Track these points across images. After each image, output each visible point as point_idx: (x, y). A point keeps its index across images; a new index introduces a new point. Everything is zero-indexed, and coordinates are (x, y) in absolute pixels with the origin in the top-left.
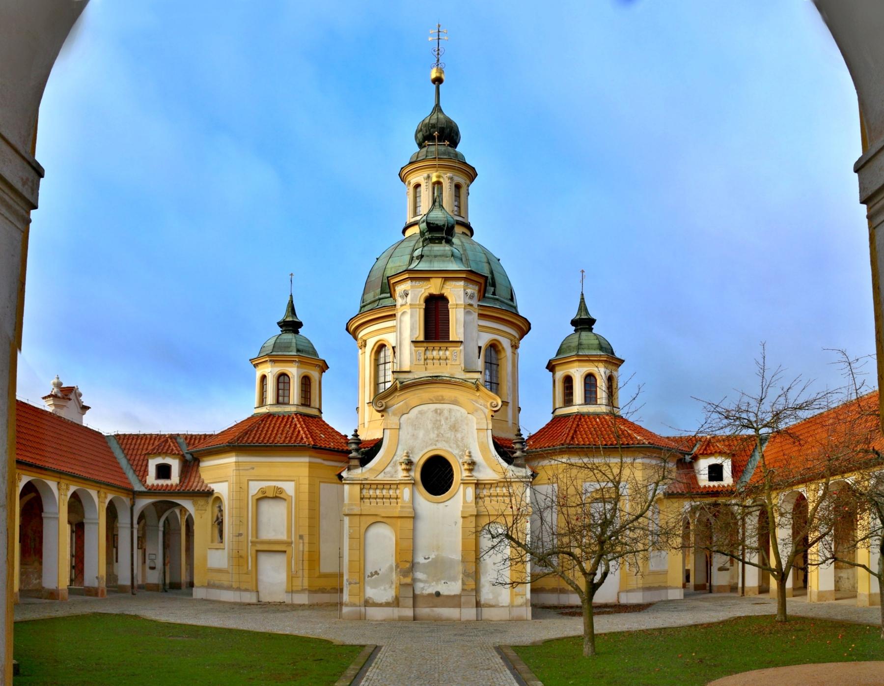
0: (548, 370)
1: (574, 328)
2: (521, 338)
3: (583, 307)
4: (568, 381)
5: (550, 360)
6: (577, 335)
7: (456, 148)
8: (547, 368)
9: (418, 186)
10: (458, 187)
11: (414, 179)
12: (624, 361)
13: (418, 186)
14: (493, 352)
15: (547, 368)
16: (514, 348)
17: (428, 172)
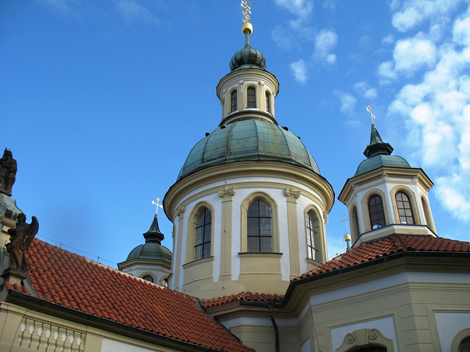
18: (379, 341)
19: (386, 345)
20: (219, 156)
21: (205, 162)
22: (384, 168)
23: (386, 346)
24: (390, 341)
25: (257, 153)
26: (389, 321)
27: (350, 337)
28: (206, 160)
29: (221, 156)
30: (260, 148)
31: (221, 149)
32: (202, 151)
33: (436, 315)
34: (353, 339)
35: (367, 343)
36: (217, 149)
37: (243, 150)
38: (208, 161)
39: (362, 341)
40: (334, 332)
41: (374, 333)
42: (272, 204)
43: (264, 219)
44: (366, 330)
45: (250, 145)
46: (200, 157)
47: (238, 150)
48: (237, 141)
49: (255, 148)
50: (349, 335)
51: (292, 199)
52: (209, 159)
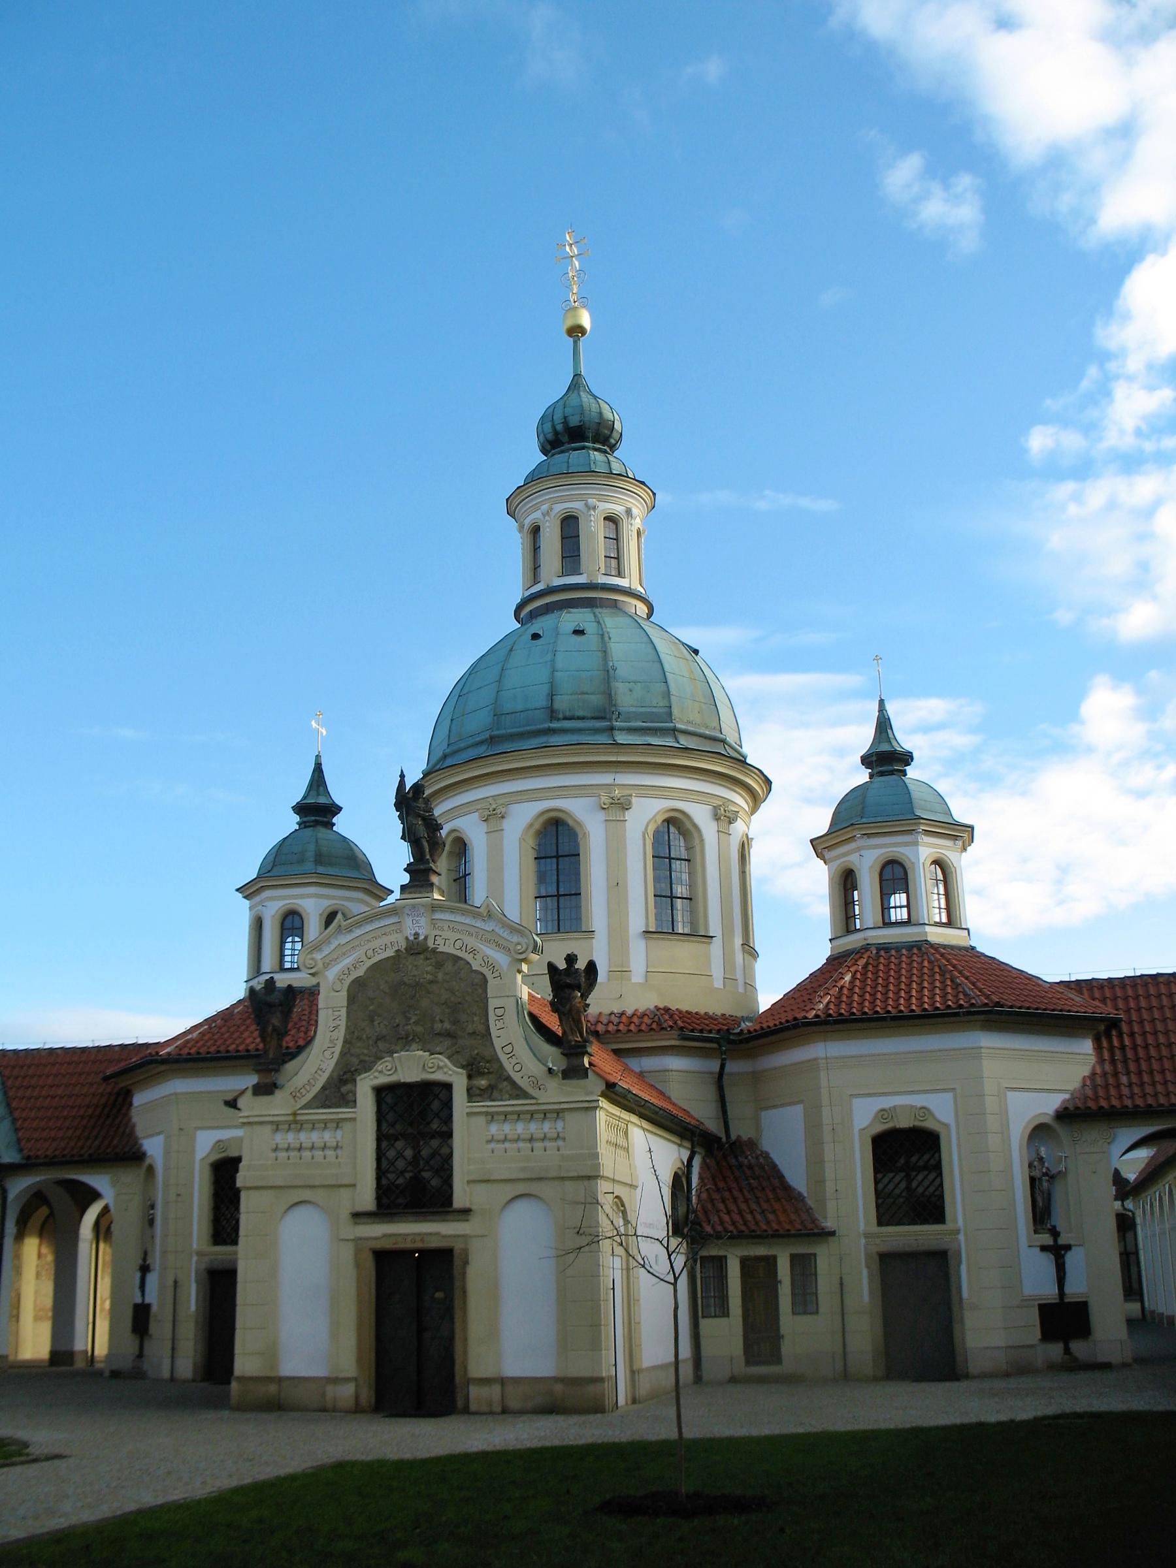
18: (929, 1125)
19: (940, 1130)
21: (559, 720)
22: (922, 821)
23: (939, 1132)
24: (947, 1126)
27: (883, 1114)
28: (561, 716)
29: (597, 714)
30: (676, 712)
31: (593, 697)
32: (544, 690)
33: (1010, 1094)
34: (890, 1116)
35: (912, 1126)
38: (565, 718)
39: (904, 1123)
40: (857, 1103)
41: (924, 1113)
42: (695, 835)
43: (678, 862)
44: (912, 1107)
45: (656, 703)
46: (542, 702)
47: (633, 709)
49: (666, 710)
50: (883, 1110)
51: (724, 824)
52: (568, 714)
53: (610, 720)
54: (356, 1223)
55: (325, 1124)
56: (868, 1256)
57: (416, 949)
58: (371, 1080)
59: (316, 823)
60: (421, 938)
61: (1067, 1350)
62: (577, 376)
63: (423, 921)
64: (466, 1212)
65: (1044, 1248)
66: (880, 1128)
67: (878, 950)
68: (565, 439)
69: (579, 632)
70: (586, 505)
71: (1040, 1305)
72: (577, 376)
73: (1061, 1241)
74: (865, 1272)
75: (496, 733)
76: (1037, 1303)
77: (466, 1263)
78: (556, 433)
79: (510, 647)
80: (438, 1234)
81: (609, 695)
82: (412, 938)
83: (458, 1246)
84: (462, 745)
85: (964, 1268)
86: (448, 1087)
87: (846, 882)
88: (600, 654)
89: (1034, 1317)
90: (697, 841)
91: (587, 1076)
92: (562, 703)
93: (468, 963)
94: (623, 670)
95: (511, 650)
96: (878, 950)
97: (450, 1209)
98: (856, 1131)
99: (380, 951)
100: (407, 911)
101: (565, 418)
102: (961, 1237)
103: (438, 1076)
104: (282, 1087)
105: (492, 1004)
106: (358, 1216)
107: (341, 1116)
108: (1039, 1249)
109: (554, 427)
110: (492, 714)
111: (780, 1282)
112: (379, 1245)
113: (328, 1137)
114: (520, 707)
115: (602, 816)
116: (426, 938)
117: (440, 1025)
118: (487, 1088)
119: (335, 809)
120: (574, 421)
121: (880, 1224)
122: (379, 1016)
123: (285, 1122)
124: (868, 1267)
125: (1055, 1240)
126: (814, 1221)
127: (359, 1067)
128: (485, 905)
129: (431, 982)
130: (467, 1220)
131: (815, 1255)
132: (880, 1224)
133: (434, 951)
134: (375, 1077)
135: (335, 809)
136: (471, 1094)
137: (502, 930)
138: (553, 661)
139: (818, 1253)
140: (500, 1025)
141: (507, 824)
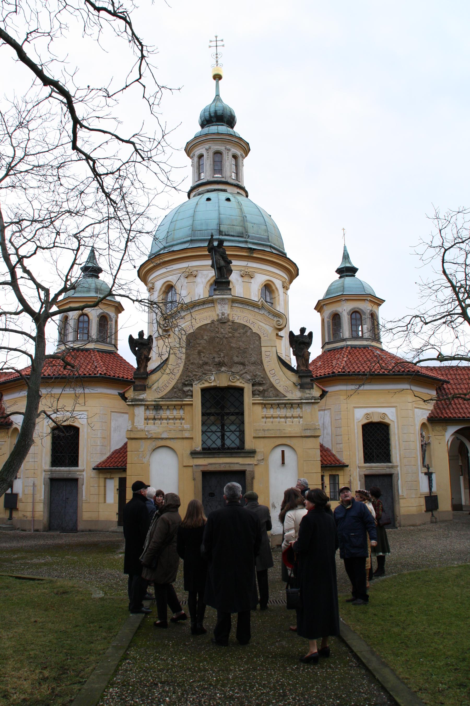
0: (316, 311)
1: (339, 276)
2: (291, 282)
3: (346, 257)
4: (336, 317)
5: (319, 301)
6: (342, 279)
7: (232, 127)
8: (315, 309)
9: (201, 156)
10: (235, 157)
11: (198, 151)
12: (384, 301)
13: (201, 156)
14: (268, 293)
15: (315, 309)
16: (285, 289)
17: (210, 145)
18: (386, 421)
20: (237, 235)
21: (223, 235)
25: (269, 244)
26: (393, 410)
28: (224, 234)
29: (239, 235)
32: (216, 222)
33: (416, 410)
36: (233, 225)
37: (258, 236)
38: (226, 235)
39: (376, 419)
40: (356, 410)
47: (254, 235)
48: (253, 225)
49: (266, 237)
52: (227, 233)
53: (245, 238)
54: (193, 458)
55: (175, 407)
56: (360, 476)
57: (223, 321)
58: (201, 384)
59: (92, 276)
60: (226, 315)
61: (432, 515)
62: (218, 95)
63: (226, 307)
64: (252, 453)
65: (426, 474)
66: (366, 421)
67: (351, 347)
68: (214, 120)
69: (228, 200)
70: (226, 148)
71: (425, 497)
72: (218, 95)
73: (430, 471)
74: (359, 483)
75: (193, 238)
76: (424, 496)
77: (253, 478)
78: (211, 117)
79: (196, 203)
80: (237, 463)
81: (245, 228)
82: (220, 315)
83: (248, 469)
84: (175, 243)
85: (399, 481)
86: (241, 390)
87: (336, 317)
88: (239, 210)
89: (423, 501)
90: (277, 295)
91: (313, 388)
92: (223, 228)
93: (250, 329)
94: (249, 218)
95: (197, 204)
96: (351, 347)
97: (243, 451)
98: (356, 421)
99: (203, 320)
100: (218, 301)
101: (216, 111)
102: (399, 469)
103: (238, 384)
104: (150, 388)
105: (263, 349)
106: (194, 454)
107: (184, 403)
108: (424, 474)
109: (210, 114)
110: (191, 230)
111: (326, 487)
112: (206, 469)
113: (176, 413)
114: (204, 228)
115: (240, 279)
116: (228, 315)
117: (237, 358)
118: (262, 391)
119: (100, 270)
120: (220, 112)
121: (365, 463)
122: (203, 352)
123: (152, 405)
124: (360, 481)
125: (428, 471)
126: (338, 460)
127: (193, 378)
128: (261, 301)
129: (231, 337)
130: (254, 457)
131: (338, 475)
132: (365, 463)
133: (233, 322)
134: (203, 383)
135: (100, 270)
136: (254, 394)
137: (268, 314)
138: (219, 210)
139: (340, 474)
140: (268, 359)
141: (198, 279)
